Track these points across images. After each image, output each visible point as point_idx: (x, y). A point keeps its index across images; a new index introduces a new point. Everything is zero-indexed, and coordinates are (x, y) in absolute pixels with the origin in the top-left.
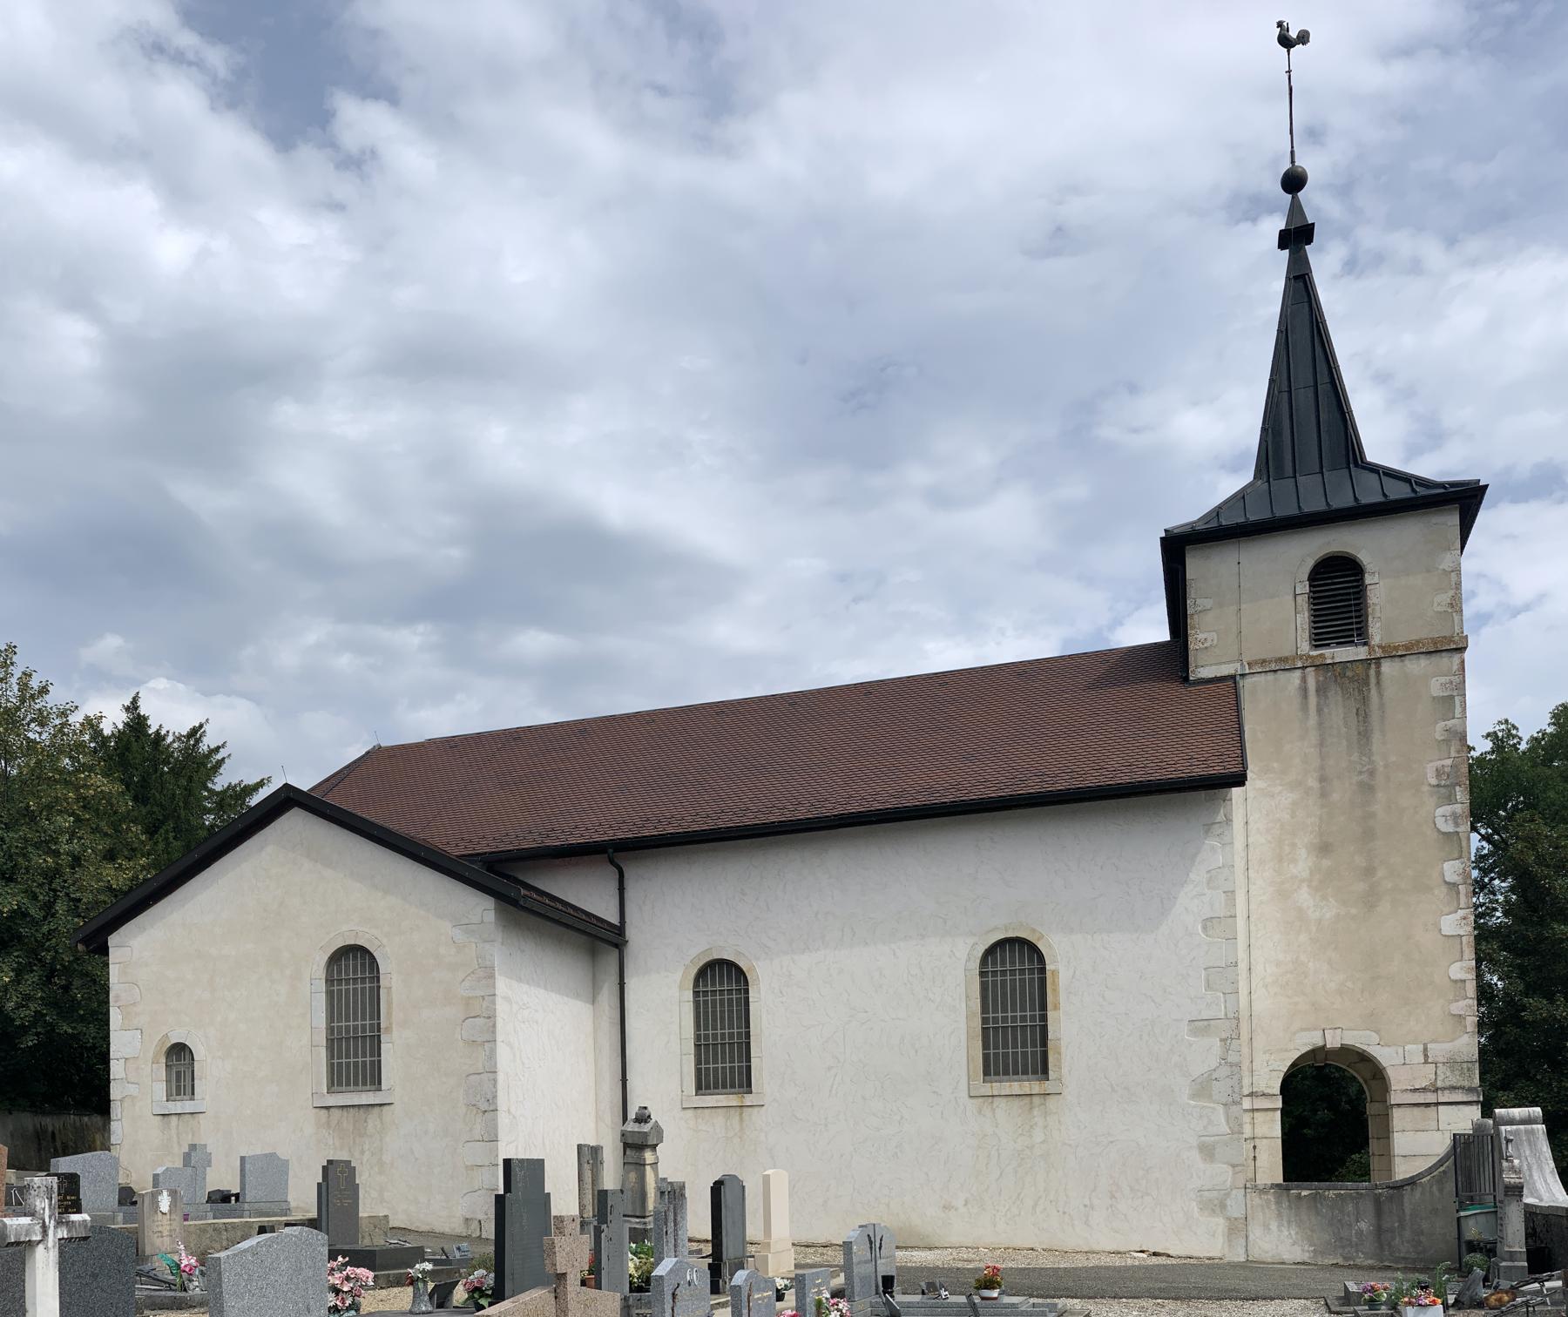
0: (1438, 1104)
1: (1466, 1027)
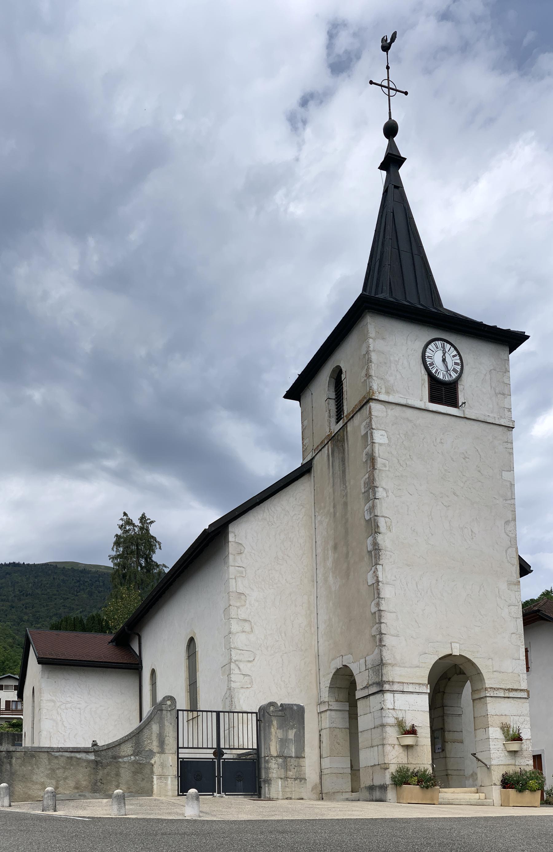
0: (370, 695)
1: (376, 643)
